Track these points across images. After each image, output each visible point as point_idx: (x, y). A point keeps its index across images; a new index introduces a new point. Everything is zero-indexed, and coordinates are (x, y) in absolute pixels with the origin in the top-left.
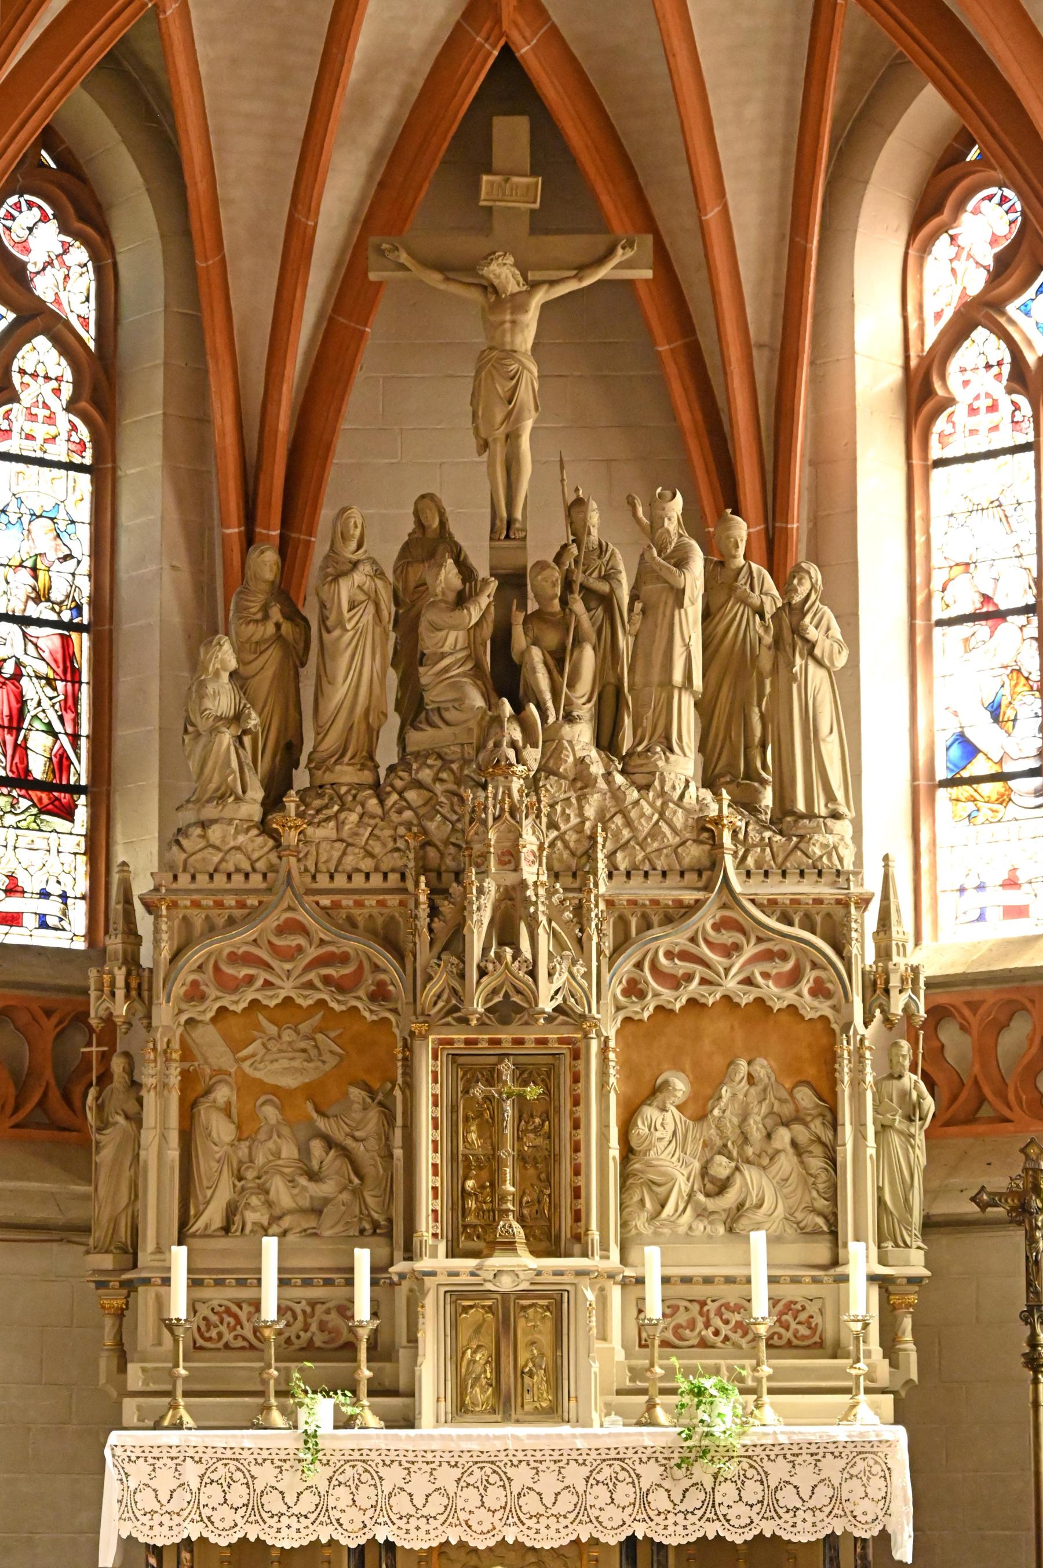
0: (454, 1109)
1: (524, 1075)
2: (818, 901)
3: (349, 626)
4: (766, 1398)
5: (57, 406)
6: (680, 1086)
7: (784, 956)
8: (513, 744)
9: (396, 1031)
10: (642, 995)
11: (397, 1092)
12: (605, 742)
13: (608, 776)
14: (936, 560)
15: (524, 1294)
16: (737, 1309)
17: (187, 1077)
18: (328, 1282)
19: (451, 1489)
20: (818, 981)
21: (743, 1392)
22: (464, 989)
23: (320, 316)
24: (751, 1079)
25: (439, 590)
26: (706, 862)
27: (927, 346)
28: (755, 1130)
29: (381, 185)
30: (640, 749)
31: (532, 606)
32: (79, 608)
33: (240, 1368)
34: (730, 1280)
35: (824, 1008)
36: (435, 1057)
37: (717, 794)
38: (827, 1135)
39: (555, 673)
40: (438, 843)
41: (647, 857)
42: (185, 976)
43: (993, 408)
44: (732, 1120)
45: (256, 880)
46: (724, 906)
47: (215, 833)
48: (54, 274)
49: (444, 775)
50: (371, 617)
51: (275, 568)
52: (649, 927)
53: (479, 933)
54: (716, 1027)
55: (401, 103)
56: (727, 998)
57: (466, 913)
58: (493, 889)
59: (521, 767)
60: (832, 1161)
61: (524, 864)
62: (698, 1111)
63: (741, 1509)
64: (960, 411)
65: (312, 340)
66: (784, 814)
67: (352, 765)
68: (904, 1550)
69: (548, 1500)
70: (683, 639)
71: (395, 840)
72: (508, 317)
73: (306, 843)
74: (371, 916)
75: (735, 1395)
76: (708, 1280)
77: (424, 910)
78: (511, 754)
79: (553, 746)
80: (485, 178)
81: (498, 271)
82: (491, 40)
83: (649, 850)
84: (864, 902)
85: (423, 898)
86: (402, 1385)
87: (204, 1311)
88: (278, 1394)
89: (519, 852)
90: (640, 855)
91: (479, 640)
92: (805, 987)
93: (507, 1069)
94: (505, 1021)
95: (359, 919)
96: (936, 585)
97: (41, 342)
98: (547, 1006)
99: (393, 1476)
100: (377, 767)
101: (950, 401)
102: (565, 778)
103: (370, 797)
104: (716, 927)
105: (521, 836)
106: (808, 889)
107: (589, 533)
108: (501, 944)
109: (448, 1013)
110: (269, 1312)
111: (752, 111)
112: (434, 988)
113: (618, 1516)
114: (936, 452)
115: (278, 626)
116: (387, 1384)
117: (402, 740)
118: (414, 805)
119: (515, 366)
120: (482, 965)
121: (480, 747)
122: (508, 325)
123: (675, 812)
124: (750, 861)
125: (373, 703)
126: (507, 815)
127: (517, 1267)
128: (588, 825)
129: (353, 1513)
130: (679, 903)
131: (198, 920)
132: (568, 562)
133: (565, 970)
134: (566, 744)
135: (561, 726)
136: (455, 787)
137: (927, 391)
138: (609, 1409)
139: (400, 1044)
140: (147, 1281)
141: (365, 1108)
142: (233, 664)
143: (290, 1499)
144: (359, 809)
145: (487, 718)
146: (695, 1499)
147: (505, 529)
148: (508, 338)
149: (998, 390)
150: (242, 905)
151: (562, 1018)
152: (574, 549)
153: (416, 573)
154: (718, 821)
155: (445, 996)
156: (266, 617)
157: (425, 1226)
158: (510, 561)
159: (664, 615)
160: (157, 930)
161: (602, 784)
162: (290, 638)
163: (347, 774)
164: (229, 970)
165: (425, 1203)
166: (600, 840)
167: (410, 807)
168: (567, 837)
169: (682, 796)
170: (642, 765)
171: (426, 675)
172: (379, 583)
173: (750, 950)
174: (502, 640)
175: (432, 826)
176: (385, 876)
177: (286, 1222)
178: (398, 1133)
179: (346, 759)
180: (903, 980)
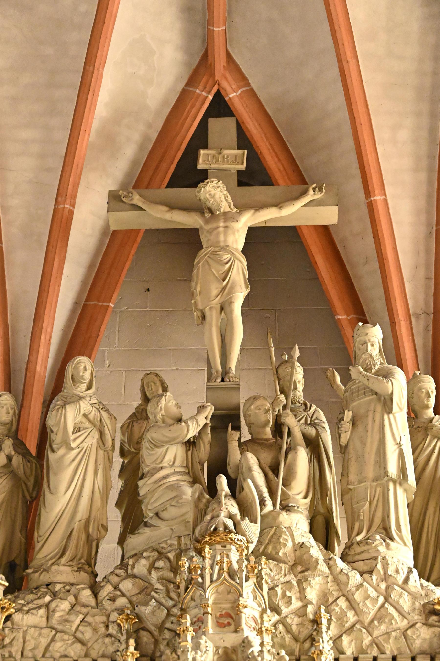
3: (73, 445)
8: (231, 517)
25: (159, 417)
30: (359, 538)
31: (246, 436)
39: (270, 474)
40: (153, 628)
41: (374, 642)
49: (160, 564)
50: (95, 441)
51: (11, 412)
55: (141, 148)
58: (211, 649)
70: (395, 439)
71: (107, 627)
72: (222, 224)
73: (12, 630)
78: (230, 524)
79: (271, 532)
80: (202, 152)
81: (213, 192)
82: (207, 89)
89: (238, 613)
90: (367, 640)
102: (285, 563)
103: (83, 589)
105: (241, 595)
107: (296, 388)
111: (404, 135)
115: (9, 458)
118: (128, 594)
119: (227, 256)
122: (221, 229)
123: (401, 595)
126: (225, 575)
128: (310, 609)
134: (284, 529)
135: (279, 514)
136: (172, 575)
144: (71, 598)
145: (204, 501)
148: (222, 238)
152: (282, 397)
159: (374, 421)
161: (323, 567)
162: (21, 472)
163: (63, 574)
166: (324, 621)
167: (123, 595)
168: (289, 621)
169: (406, 580)
170: (362, 552)
171: (144, 487)
179: (63, 561)
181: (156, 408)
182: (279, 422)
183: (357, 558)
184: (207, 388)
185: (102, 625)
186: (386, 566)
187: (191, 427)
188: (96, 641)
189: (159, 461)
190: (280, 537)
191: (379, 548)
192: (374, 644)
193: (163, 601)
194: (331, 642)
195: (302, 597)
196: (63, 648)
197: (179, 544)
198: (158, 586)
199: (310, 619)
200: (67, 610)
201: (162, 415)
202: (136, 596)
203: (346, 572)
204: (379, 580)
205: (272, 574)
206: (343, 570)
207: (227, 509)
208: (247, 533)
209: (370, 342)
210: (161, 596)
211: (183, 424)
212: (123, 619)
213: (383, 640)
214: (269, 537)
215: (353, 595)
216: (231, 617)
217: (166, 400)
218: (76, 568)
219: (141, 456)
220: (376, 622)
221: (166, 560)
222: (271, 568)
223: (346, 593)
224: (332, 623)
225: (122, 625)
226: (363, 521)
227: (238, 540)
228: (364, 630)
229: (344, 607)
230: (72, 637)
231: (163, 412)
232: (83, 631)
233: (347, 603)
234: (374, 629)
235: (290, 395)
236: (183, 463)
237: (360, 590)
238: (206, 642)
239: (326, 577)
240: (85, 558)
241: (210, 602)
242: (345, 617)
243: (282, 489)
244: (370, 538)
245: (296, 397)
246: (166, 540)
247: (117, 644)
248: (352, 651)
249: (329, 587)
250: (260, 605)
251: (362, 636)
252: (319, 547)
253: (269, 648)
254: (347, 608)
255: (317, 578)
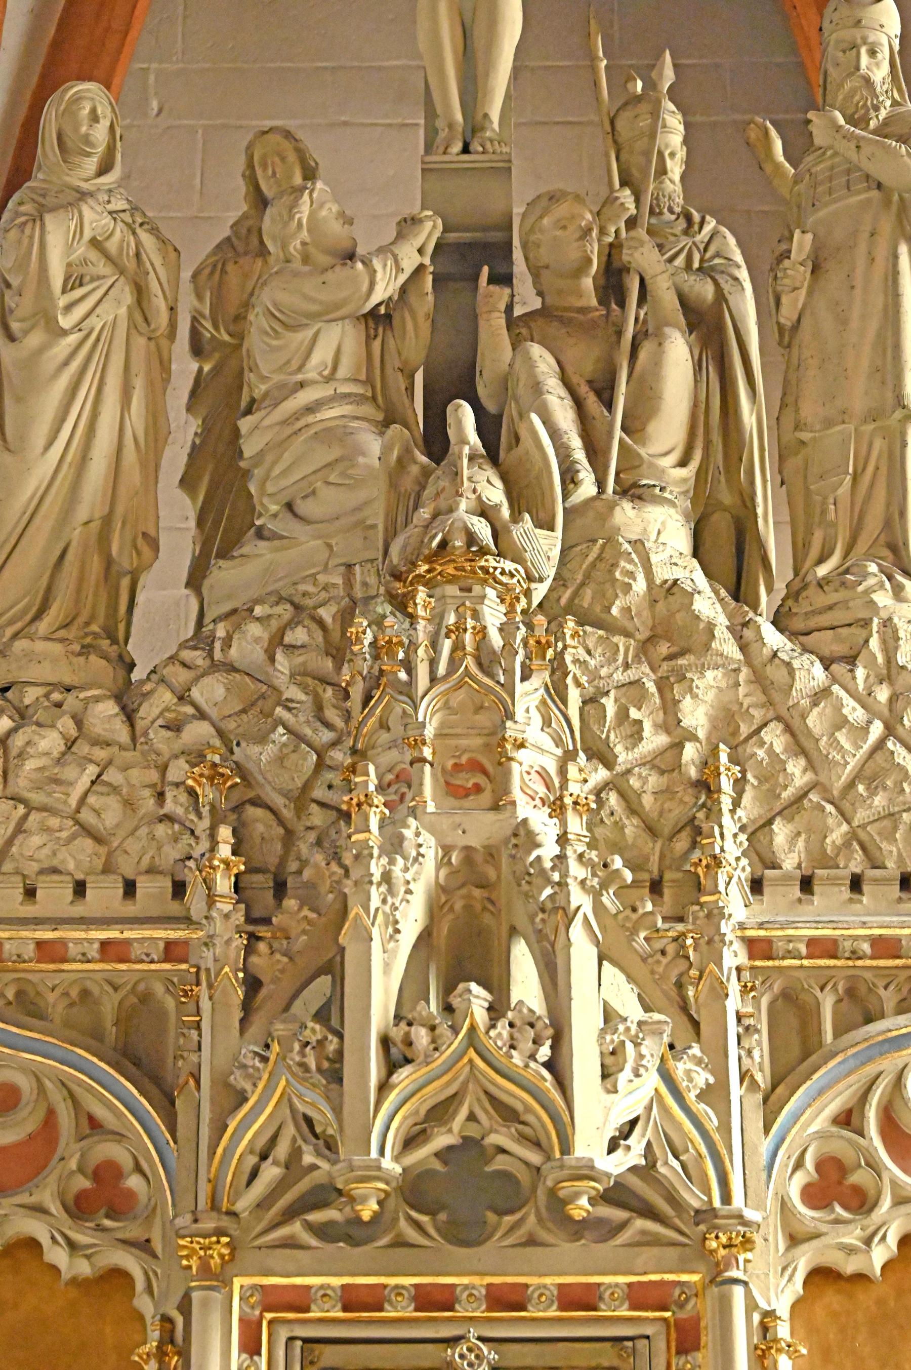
3: (65, 322)
8: (484, 511)
9: (145, 1305)
10: (862, 1202)
22: (338, 1111)
25: (295, 246)
30: (822, 571)
31: (528, 300)
36: (251, 1347)
39: (592, 402)
40: (279, 801)
49: (298, 635)
50: (123, 311)
53: (387, 966)
57: (348, 887)
58: (431, 853)
67: (62, 640)
71: (161, 796)
74: (85, 993)
78: (483, 529)
79: (593, 554)
83: (861, 816)
89: (504, 762)
90: (838, 833)
91: (394, 362)
94: (465, 1234)
95: (51, 997)
102: (627, 635)
103: (97, 699)
107: (662, 171)
109: (289, 1215)
112: (250, 1129)
118: (213, 713)
120: (397, 1034)
125: (120, 510)
126: (469, 661)
128: (690, 752)
133: (652, 1064)
135: (612, 506)
136: (329, 664)
139: (154, 1335)
144: (67, 724)
145: (414, 470)
151: (641, 1223)
152: (626, 196)
155: (282, 1150)
166: (726, 785)
167: (202, 715)
168: (634, 782)
170: (830, 608)
172: (146, 238)
175: (260, 756)
176: (130, 889)
179: (43, 627)
181: (286, 224)
182: (616, 264)
183: (813, 623)
184: (423, 170)
185: (147, 793)
186: (891, 642)
187: (379, 275)
188: (132, 833)
189: (295, 365)
190: (615, 565)
191: (875, 597)
192: (855, 843)
193: (308, 731)
194: (743, 837)
195: (670, 720)
196: (46, 851)
197: (349, 583)
198: (294, 692)
199: (690, 778)
200: (56, 754)
201: (304, 244)
202: (236, 718)
203: (786, 658)
204: (872, 679)
205: (592, 663)
206: (779, 654)
207: (474, 491)
208: (528, 556)
209: (865, 43)
210: (302, 719)
211: (359, 265)
212: (201, 775)
213: (879, 834)
214: (584, 566)
215: (804, 717)
216: (485, 772)
217: (312, 202)
218: (76, 647)
219: (248, 350)
220: (861, 788)
221: (314, 626)
222: (591, 646)
223: (784, 713)
224: (748, 788)
225: (199, 791)
226: (834, 525)
227: (503, 573)
228: (829, 808)
229: (778, 748)
230: (71, 823)
231: (305, 234)
232: (97, 807)
233: (788, 736)
234: (857, 804)
235: (646, 191)
236: (358, 369)
237: (822, 704)
238: (418, 834)
239: (735, 670)
240: (101, 619)
241: (429, 732)
242: (781, 775)
243: (621, 441)
244: (854, 570)
245: (664, 196)
246: (314, 575)
247: (187, 839)
248: (796, 861)
249: (741, 697)
250: (558, 742)
251: (825, 823)
252: (716, 592)
253: (581, 848)
254: (786, 750)
255: (710, 674)
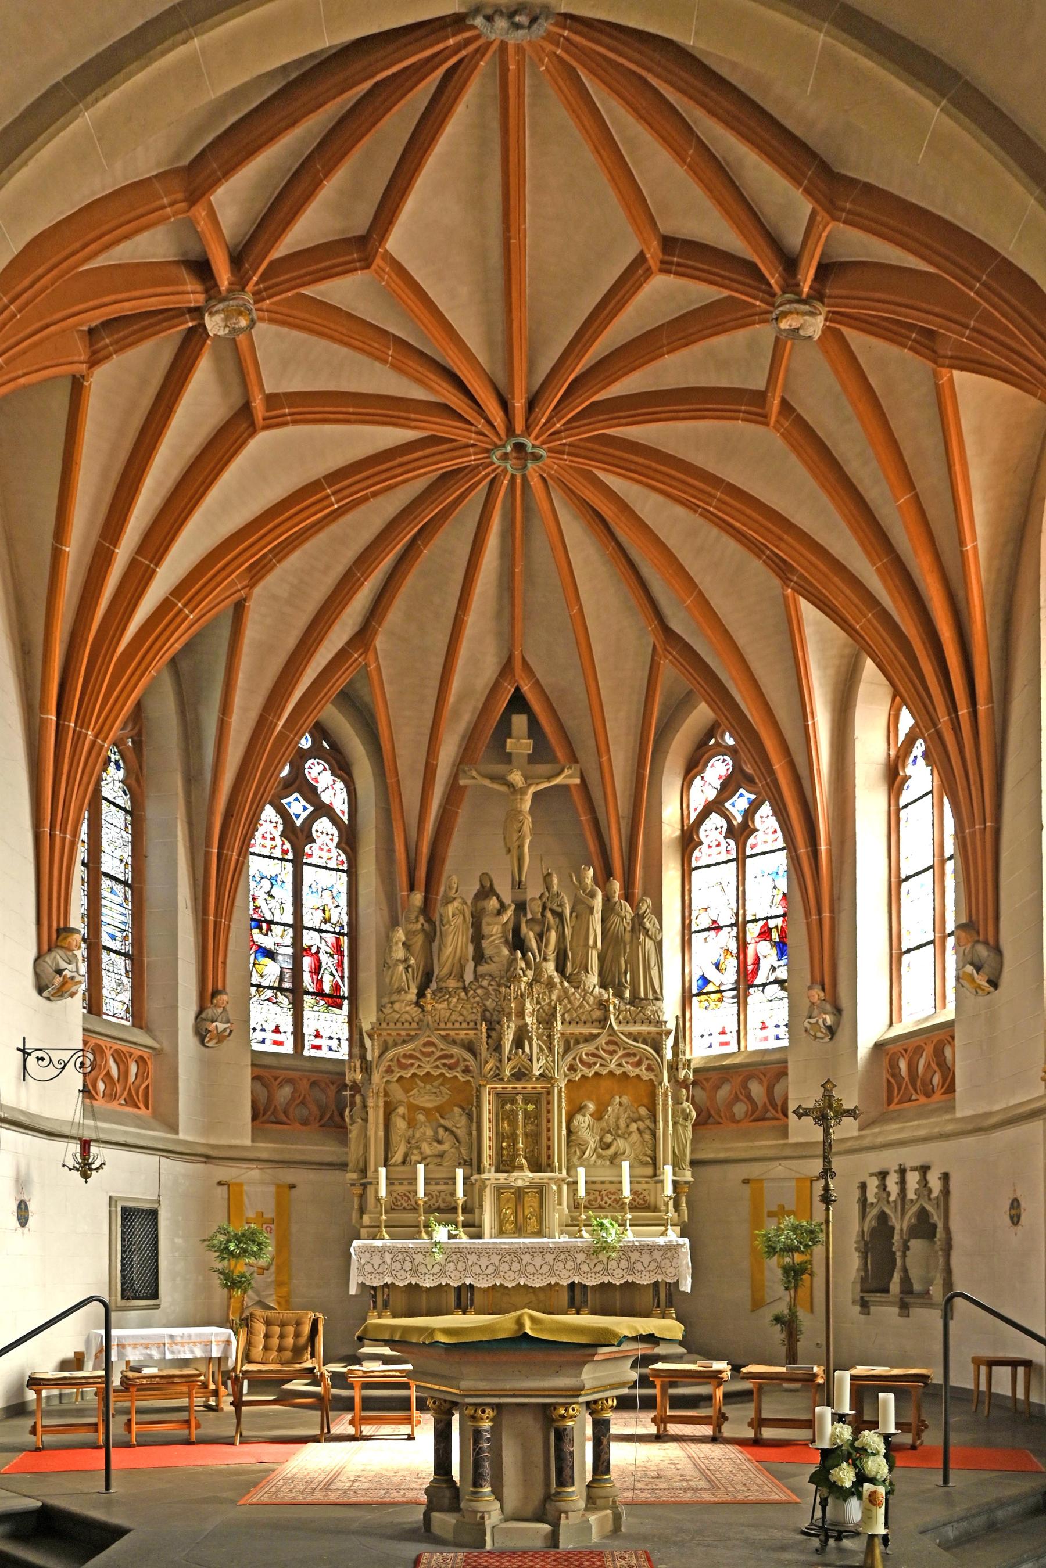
0: (497, 1114)
1: (526, 1101)
2: (649, 1033)
4: (628, 1227)
5: (332, 845)
6: (591, 1107)
7: (635, 1055)
8: (522, 969)
10: (575, 1071)
11: (474, 1109)
12: (560, 969)
13: (561, 983)
14: (693, 907)
15: (528, 1187)
16: (615, 1193)
17: (387, 1104)
18: (446, 1184)
19: (497, 1264)
20: (649, 1065)
21: (620, 1225)
23: (440, 806)
24: (620, 1104)
26: (602, 1017)
27: (692, 820)
28: (622, 1123)
29: (465, 750)
31: (529, 916)
32: (342, 927)
33: (409, 1217)
34: (611, 1182)
35: (651, 1076)
37: (606, 990)
38: (652, 1126)
41: (578, 1016)
42: (385, 1064)
43: (718, 845)
44: (612, 1121)
45: (414, 1025)
46: (610, 1035)
47: (397, 1006)
48: (330, 792)
52: (578, 1043)
54: (605, 1084)
56: (611, 1072)
59: (524, 979)
60: (654, 1135)
61: (527, 1018)
62: (598, 1116)
63: (619, 1271)
64: (704, 847)
65: (437, 815)
66: (635, 1000)
68: (686, 1286)
69: (538, 1268)
75: (616, 1225)
76: (603, 1182)
77: (484, 1035)
78: (521, 973)
79: (539, 971)
84: (668, 1033)
85: (484, 1030)
86: (477, 1223)
87: (395, 1195)
88: (425, 1227)
90: (575, 1015)
92: (643, 1067)
93: (520, 1098)
96: (693, 917)
97: (325, 819)
98: (537, 1073)
99: (472, 1258)
100: (464, 981)
101: (701, 843)
104: (606, 1044)
106: (645, 1028)
108: (517, 1048)
110: (421, 1193)
113: (567, 1274)
114: (694, 865)
116: (470, 1222)
117: (475, 971)
121: (508, 970)
124: (621, 1017)
127: (524, 1177)
129: (456, 1273)
130: (591, 1034)
131: (390, 1041)
132: (545, 899)
137: (691, 839)
138: (562, 1232)
140: (371, 1183)
141: (461, 1115)
142: (404, 939)
143: (430, 1268)
146: (600, 1267)
147: (518, 885)
149: (721, 838)
150: (408, 1035)
153: (480, 905)
154: (608, 1001)
156: (417, 921)
157: (486, 1162)
158: (521, 898)
160: (373, 1045)
163: (452, 983)
164: (403, 1061)
165: (486, 1152)
171: (485, 944)
173: (621, 1053)
174: (517, 930)
177: (428, 1160)
178: (474, 1125)
180: (684, 1065)
195: (550, 998)
